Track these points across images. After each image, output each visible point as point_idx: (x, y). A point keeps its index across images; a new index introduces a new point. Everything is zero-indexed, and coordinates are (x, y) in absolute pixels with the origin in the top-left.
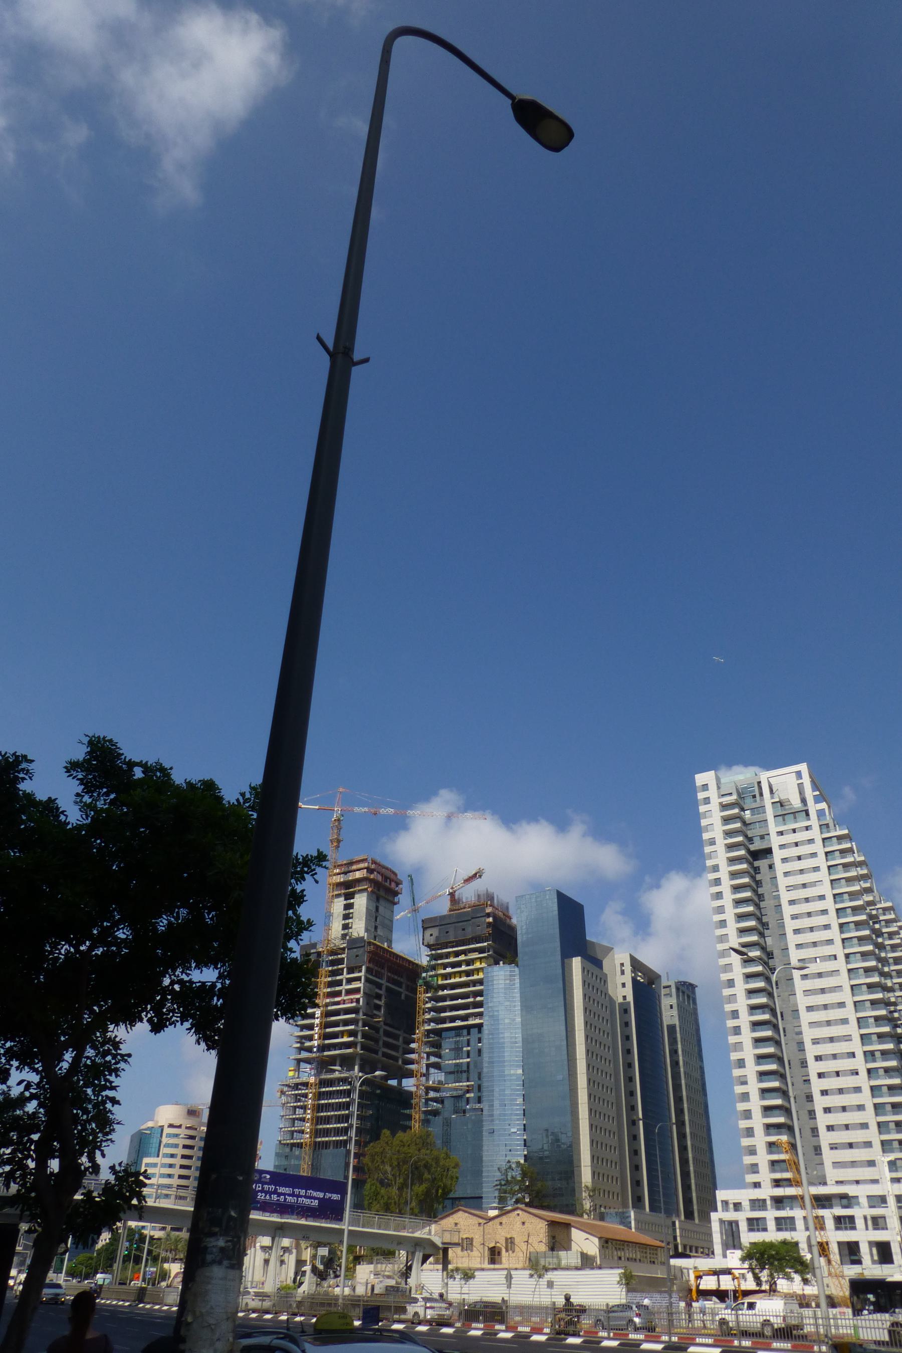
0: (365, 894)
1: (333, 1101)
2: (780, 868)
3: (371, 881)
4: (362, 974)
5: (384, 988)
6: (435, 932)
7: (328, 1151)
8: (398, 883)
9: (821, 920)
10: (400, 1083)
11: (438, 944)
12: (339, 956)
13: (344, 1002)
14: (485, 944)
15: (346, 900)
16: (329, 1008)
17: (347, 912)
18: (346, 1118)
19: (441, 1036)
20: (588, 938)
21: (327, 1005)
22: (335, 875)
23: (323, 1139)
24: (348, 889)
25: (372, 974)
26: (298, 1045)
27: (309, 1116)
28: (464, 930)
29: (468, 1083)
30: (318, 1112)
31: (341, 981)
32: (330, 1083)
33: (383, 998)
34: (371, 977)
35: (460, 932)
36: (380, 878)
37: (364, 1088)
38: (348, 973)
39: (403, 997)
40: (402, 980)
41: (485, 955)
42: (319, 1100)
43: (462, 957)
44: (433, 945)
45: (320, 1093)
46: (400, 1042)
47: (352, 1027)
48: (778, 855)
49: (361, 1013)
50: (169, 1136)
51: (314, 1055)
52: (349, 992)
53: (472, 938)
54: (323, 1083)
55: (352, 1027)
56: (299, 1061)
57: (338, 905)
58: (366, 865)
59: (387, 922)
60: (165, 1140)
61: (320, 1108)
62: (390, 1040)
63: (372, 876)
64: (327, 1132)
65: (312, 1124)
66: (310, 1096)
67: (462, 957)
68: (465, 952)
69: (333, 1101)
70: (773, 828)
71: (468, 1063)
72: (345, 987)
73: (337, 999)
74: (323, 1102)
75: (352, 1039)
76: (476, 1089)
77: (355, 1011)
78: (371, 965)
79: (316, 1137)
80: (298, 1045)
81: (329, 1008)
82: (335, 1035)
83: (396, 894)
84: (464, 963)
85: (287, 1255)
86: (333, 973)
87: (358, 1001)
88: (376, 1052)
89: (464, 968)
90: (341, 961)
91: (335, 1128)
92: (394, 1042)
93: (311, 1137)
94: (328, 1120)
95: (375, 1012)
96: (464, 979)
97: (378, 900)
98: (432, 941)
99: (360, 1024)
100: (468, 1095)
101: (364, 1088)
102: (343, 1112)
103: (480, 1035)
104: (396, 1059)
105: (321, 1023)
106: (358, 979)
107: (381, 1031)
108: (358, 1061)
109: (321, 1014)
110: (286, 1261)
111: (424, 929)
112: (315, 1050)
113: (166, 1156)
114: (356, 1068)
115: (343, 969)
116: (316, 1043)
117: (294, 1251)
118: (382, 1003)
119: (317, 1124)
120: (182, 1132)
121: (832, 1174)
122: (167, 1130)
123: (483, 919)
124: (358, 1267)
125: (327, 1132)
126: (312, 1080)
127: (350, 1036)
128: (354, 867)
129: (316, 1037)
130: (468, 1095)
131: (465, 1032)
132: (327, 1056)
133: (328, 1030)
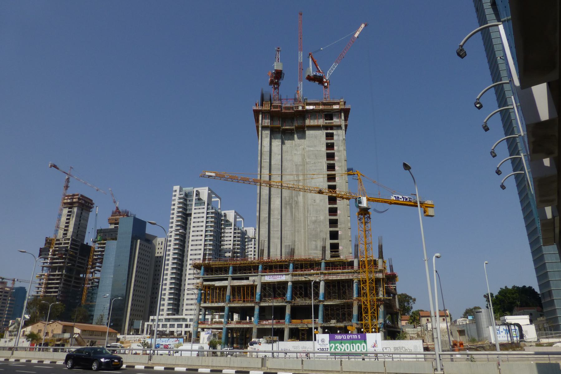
2: (193, 220)
8: (92, 204)
9: (200, 238)
20: (146, 232)
36: (83, 202)
48: (193, 215)
56: (43, 267)
57: (65, 211)
70: (193, 207)
83: (91, 208)
97: (82, 210)
121: (185, 312)
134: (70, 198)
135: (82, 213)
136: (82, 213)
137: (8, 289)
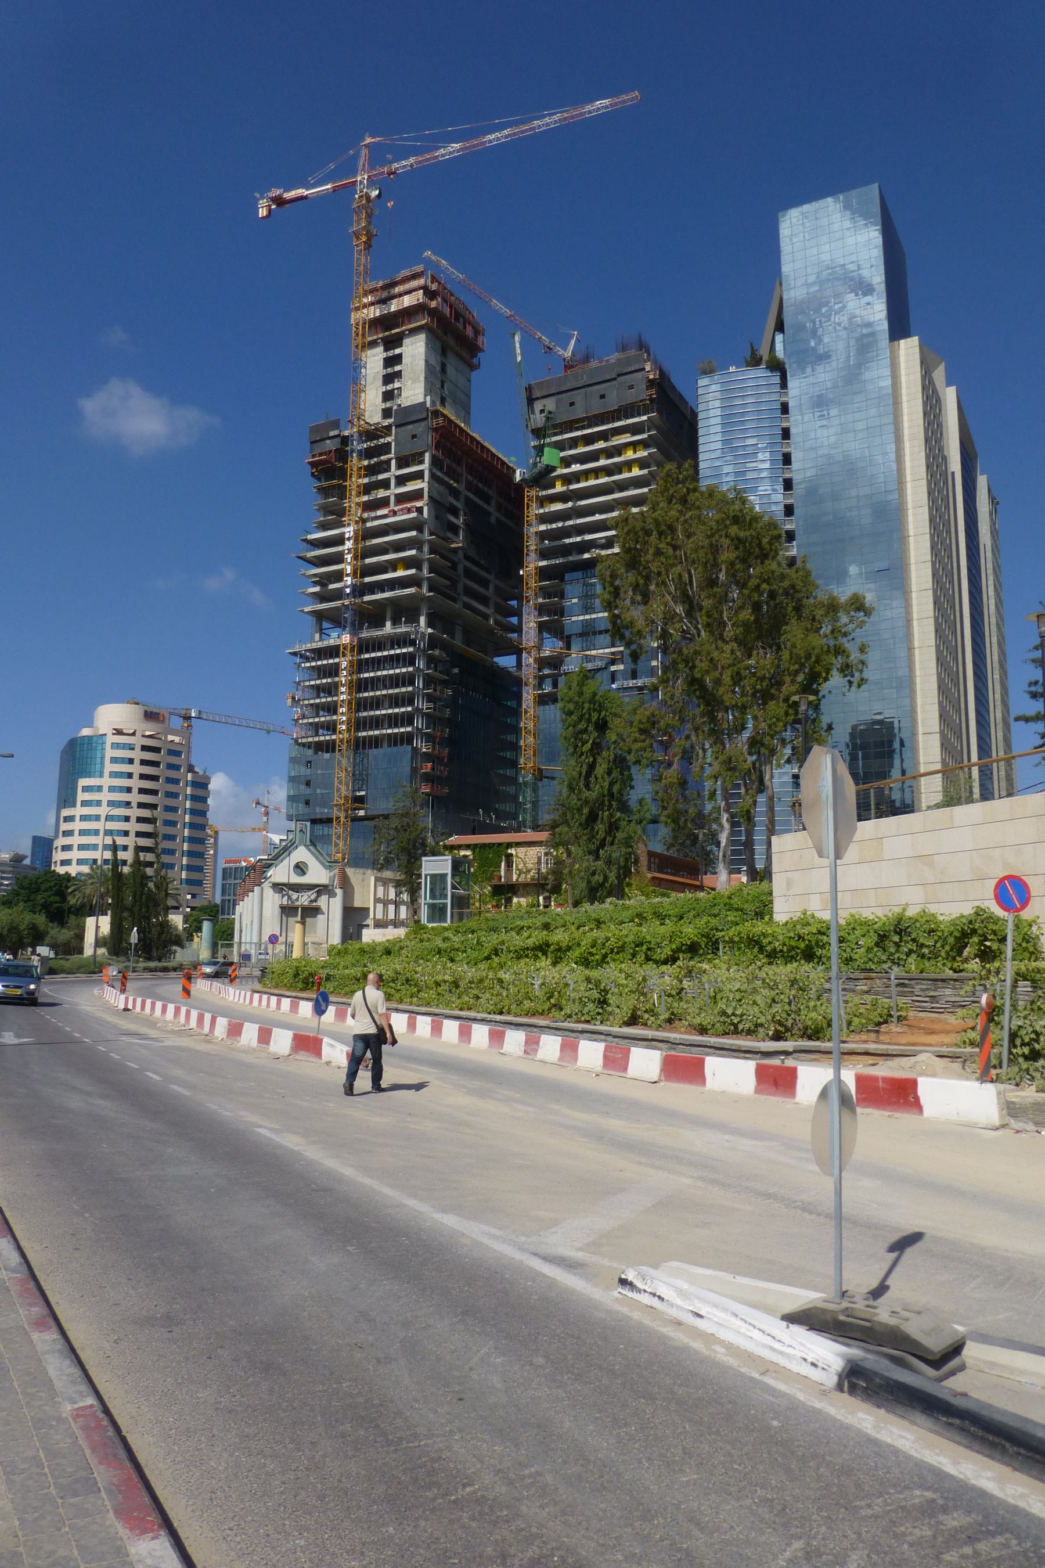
0: (421, 338)
1: (385, 673)
3: (433, 313)
4: (425, 466)
6: (550, 404)
7: (380, 751)
8: (477, 332)
11: (555, 426)
12: (382, 440)
13: (395, 513)
14: (645, 418)
15: (386, 350)
16: (369, 524)
17: (389, 387)
18: (409, 700)
19: (562, 580)
22: (365, 306)
23: (371, 733)
24: (389, 331)
25: (441, 470)
27: (343, 697)
28: (603, 397)
29: (613, 650)
30: (359, 691)
31: (388, 480)
32: (378, 644)
34: (439, 473)
36: (447, 311)
38: (399, 467)
39: (493, 520)
40: (490, 492)
41: (645, 436)
42: (360, 671)
43: (601, 445)
45: (360, 662)
47: (413, 552)
50: (116, 746)
52: (401, 499)
53: (618, 411)
54: (364, 646)
55: (413, 552)
57: (374, 360)
58: (421, 282)
60: (109, 753)
61: (362, 685)
62: (476, 586)
63: (433, 304)
64: (376, 723)
65: (350, 709)
66: (344, 664)
67: (601, 445)
68: (604, 436)
69: (385, 673)
73: (380, 513)
74: (366, 675)
75: (413, 571)
77: (416, 525)
78: (440, 454)
80: (317, 589)
81: (369, 524)
82: (382, 568)
86: (371, 470)
87: (420, 510)
88: (455, 600)
89: (602, 462)
90: (386, 448)
91: (390, 715)
92: (482, 590)
93: (349, 730)
95: (450, 535)
97: (444, 352)
99: (426, 549)
100: (613, 668)
101: (437, 652)
104: (486, 617)
105: (356, 549)
106: (419, 475)
107: (460, 569)
110: (324, 908)
112: (348, 591)
113: (114, 775)
114: (422, 620)
115: (390, 460)
116: (349, 580)
117: (339, 892)
118: (460, 521)
119: (358, 710)
120: (138, 741)
122: (111, 739)
123: (639, 375)
124: (774, 839)
125: (376, 723)
126: (346, 639)
127: (407, 568)
129: (349, 569)
130: (613, 668)
133: (368, 561)
137: (177, 739)
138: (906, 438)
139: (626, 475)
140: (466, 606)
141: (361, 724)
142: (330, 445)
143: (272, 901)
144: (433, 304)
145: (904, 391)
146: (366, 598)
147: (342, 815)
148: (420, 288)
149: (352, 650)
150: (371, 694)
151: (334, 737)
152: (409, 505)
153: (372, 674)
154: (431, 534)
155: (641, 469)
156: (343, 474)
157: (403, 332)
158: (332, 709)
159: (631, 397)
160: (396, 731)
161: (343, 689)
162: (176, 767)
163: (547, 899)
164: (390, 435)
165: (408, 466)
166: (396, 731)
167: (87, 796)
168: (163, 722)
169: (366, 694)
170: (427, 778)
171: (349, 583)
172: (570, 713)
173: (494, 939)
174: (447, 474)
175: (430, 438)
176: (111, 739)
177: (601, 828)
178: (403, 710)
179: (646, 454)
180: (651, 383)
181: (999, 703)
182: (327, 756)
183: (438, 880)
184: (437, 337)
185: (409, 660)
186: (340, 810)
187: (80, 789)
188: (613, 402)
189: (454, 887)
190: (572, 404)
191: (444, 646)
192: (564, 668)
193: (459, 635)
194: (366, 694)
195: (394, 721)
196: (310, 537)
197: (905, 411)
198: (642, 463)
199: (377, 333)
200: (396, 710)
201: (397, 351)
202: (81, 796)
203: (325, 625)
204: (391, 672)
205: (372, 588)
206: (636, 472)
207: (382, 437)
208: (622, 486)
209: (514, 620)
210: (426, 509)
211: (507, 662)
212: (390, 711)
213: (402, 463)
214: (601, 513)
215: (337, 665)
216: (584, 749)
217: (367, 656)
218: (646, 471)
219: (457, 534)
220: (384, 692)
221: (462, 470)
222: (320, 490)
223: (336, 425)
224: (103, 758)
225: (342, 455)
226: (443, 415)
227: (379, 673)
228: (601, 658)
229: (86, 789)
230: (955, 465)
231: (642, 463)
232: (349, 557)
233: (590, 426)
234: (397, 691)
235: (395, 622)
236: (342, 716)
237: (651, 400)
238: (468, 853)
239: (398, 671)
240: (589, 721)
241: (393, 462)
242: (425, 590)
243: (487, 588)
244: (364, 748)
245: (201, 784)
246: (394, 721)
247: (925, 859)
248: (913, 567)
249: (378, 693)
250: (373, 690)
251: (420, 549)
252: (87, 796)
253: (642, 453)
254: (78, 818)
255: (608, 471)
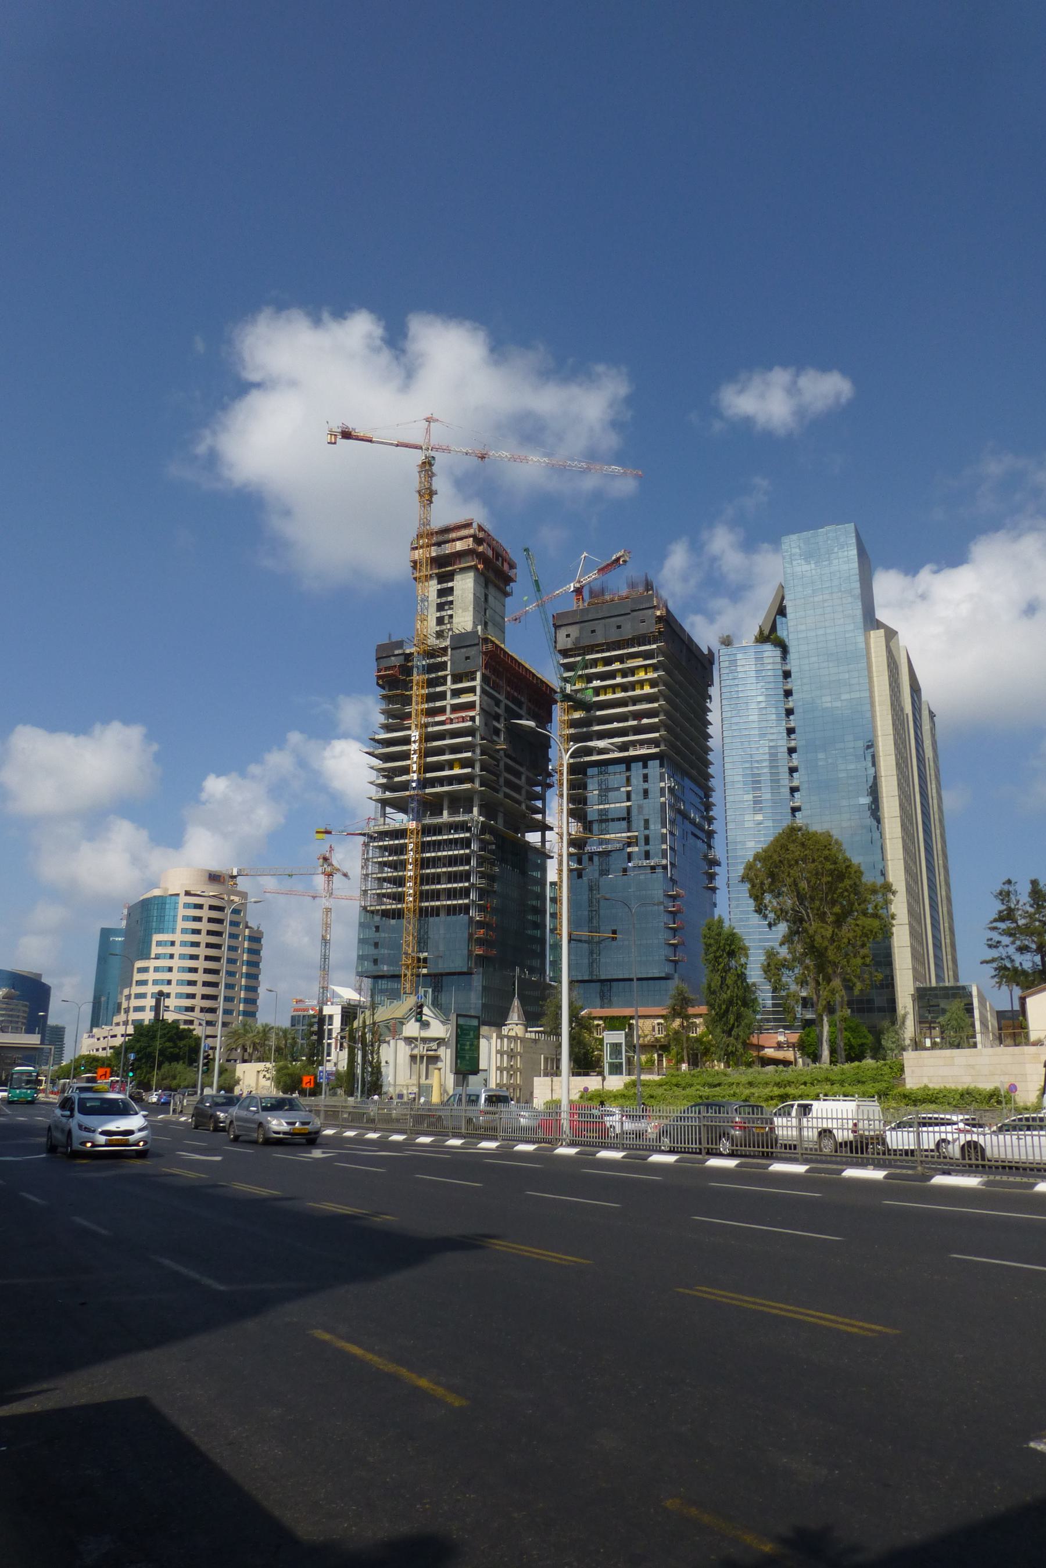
1: (445, 853)
3: (481, 556)
4: (477, 683)
5: (502, 706)
6: (574, 631)
8: (512, 566)
10: (524, 836)
12: (439, 659)
13: (451, 721)
14: (654, 646)
15: (439, 583)
16: (430, 729)
18: (465, 876)
19: (585, 774)
21: (426, 725)
23: (433, 904)
24: (444, 568)
25: (488, 685)
26: (384, 781)
27: (412, 873)
29: (629, 834)
30: (422, 868)
32: (437, 830)
33: (502, 720)
34: (487, 688)
35: (614, 630)
36: (490, 553)
37: (571, 806)
38: (454, 682)
41: (655, 661)
42: (423, 852)
43: (617, 666)
44: (571, 650)
45: (423, 843)
46: (522, 782)
47: (469, 754)
49: (478, 737)
50: (187, 906)
51: (412, 792)
52: (455, 708)
53: (633, 639)
54: (427, 830)
55: (469, 754)
58: (471, 531)
59: (498, 618)
60: (182, 912)
61: (424, 863)
63: (481, 549)
64: (436, 895)
65: (415, 883)
67: (617, 666)
68: (621, 659)
69: (445, 853)
71: (629, 808)
72: (450, 701)
73: (438, 719)
74: (428, 855)
76: (642, 841)
77: (470, 732)
78: (487, 673)
79: (421, 901)
80: (384, 781)
81: (430, 729)
82: (440, 766)
83: (508, 580)
84: (619, 674)
85: (442, 1049)
86: (431, 683)
87: (473, 719)
89: (619, 680)
90: (443, 666)
93: (415, 901)
94: (436, 879)
95: (495, 738)
96: (620, 695)
97: (486, 586)
98: (568, 643)
99: (478, 751)
100: (629, 850)
101: (487, 837)
102: (461, 868)
103: (645, 771)
104: (519, 803)
105: (420, 749)
106: (472, 690)
107: (502, 764)
108: (476, 802)
109: (420, 737)
110: (443, 1057)
111: (557, 627)
112: (414, 785)
113: (184, 931)
114: (475, 810)
116: (415, 776)
119: (422, 884)
123: (650, 611)
125: (436, 895)
126: (413, 825)
127: (462, 767)
128: (453, 535)
129: (415, 767)
130: (629, 850)
131: (623, 767)
132: (428, 794)
133: (429, 759)
134: (434, 540)
135: (486, 596)
136: (486, 596)
138: (877, 704)
139: (638, 692)
140: (507, 796)
141: (424, 896)
142: (394, 661)
143: (404, 1051)
144: (481, 549)
145: (874, 669)
146: (428, 791)
147: (409, 974)
148: (471, 536)
149: (417, 834)
150: (433, 871)
151: (399, 906)
152: (463, 714)
153: (433, 854)
154: (482, 739)
155: (652, 687)
156: (407, 685)
157: (455, 570)
158: (400, 882)
159: (643, 629)
160: (455, 902)
161: (410, 867)
162: (234, 924)
163: (660, 1056)
164: (446, 655)
165: (461, 681)
166: (455, 902)
167: (161, 950)
168: (223, 883)
169: (428, 871)
170: (480, 942)
171: (415, 778)
172: (710, 945)
173: (747, 1092)
174: (493, 688)
175: (480, 660)
176: (183, 899)
177: (732, 1018)
178: (461, 885)
179: (656, 675)
180: (660, 619)
181: (943, 883)
182: (393, 922)
183: (616, 1048)
184: (482, 574)
185: (466, 843)
186: (408, 968)
187: (154, 943)
188: (628, 633)
189: (626, 1051)
190: (593, 631)
191: (492, 831)
192: (588, 849)
193: (500, 821)
194: (428, 871)
195: (451, 894)
196: (377, 737)
197: (876, 684)
198: (653, 683)
199: (431, 569)
200: (455, 885)
201: (450, 584)
202: (155, 950)
203: (388, 810)
204: (450, 853)
205: (432, 783)
206: (647, 690)
207: (439, 656)
208: (635, 700)
209: (539, 804)
210: (477, 718)
211: (533, 838)
212: (449, 886)
213: (457, 678)
214: (619, 722)
215: (405, 846)
216: (720, 967)
217: (429, 839)
218: (656, 690)
219: (498, 735)
220: (444, 870)
221: (502, 683)
222: (384, 697)
223: (400, 644)
224: (175, 916)
225: (407, 671)
226: (493, 642)
227: (440, 854)
228: (619, 842)
229: (159, 944)
230: (908, 709)
231: (653, 683)
232: (415, 757)
233: (608, 650)
234: (455, 869)
235: (453, 812)
236: (409, 889)
237: (660, 632)
238: (601, 1022)
239: (456, 852)
240: (724, 950)
241: (449, 678)
242: (477, 785)
243: (520, 779)
244: (426, 916)
245: (256, 939)
246: (451, 894)
247: (972, 1066)
248: (885, 800)
249: (439, 870)
250: (434, 867)
251: (474, 752)
252: (161, 950)
253: (652, 675)
254: (151, 970)
255: (624, 688)
